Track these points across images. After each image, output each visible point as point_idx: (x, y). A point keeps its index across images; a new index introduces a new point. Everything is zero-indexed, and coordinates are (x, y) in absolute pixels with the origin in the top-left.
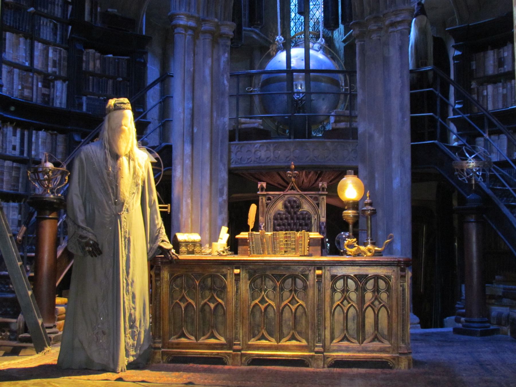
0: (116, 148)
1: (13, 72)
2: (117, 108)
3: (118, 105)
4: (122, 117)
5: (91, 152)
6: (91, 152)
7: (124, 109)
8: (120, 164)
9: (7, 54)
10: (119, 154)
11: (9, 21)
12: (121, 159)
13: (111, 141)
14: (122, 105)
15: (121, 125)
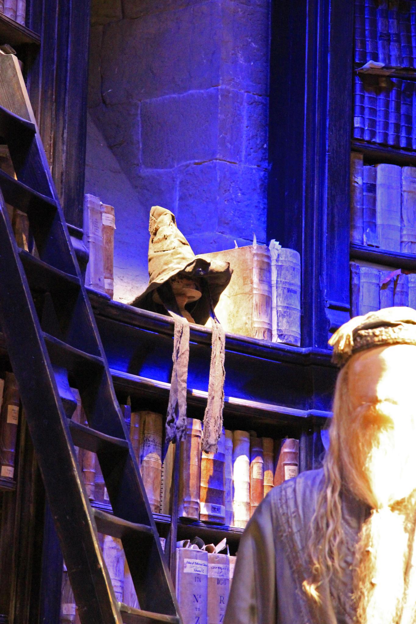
0: (360, 483)
1: (405, 285)
2: (363, 344)
3: (363, 332)
4: (378, 369)
5: (291, 503)
6: (291, 503)
7: (385, 344)
8: (368, 536)
9: (379, 230)
10: (371, 503)
11: (379, 130)
12: (375, 518)
13: (346, 458)
14: (377, 331)
15: (375, 401)
